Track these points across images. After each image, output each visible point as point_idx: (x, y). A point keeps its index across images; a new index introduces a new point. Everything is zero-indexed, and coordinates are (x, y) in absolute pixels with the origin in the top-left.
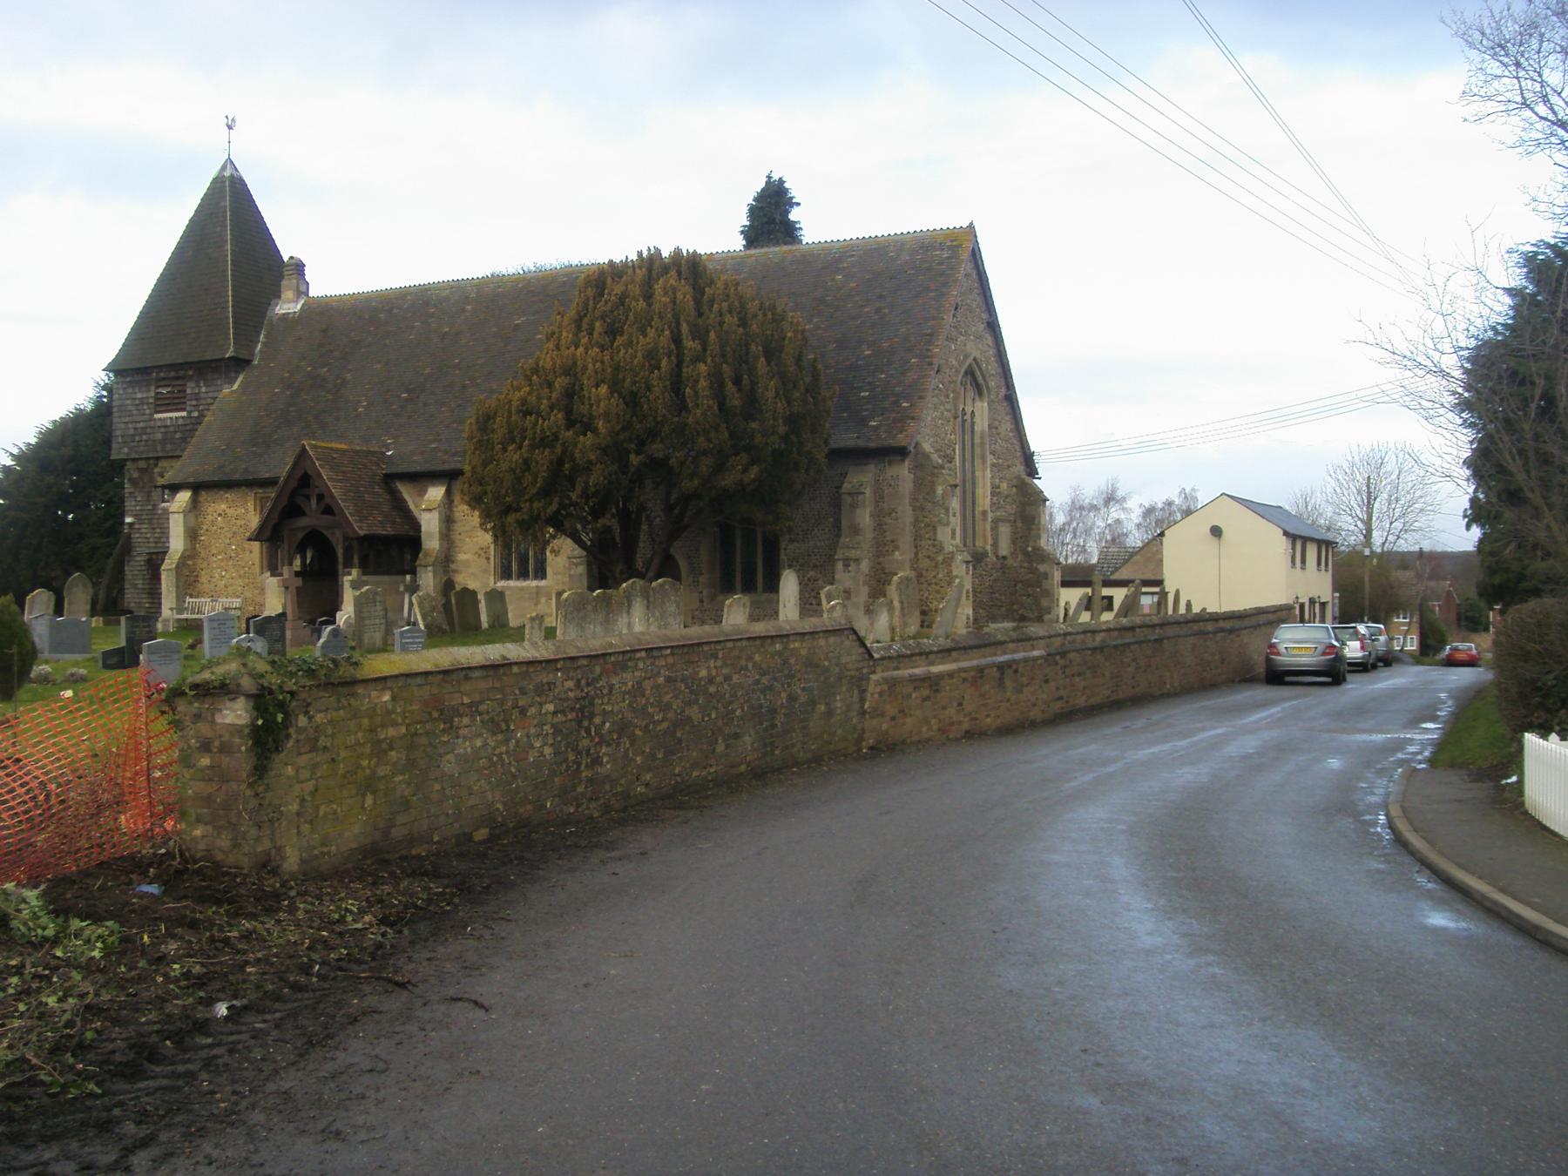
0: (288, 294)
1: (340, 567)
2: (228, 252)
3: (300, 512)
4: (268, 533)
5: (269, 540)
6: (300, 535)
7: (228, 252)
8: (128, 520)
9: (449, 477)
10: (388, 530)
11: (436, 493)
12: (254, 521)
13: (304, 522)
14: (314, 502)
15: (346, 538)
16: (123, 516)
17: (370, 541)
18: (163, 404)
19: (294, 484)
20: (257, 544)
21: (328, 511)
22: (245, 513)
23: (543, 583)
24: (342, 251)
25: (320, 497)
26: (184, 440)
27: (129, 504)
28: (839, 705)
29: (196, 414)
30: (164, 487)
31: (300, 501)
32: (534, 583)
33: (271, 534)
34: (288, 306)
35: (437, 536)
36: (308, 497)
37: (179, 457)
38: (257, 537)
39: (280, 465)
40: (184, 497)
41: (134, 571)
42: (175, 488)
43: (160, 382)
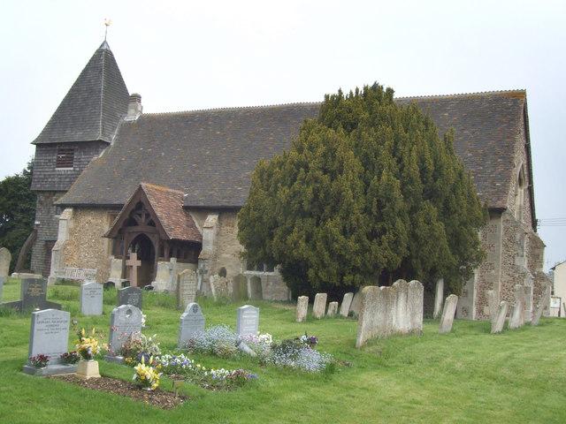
0: (131, 111)
1: (156, 256)
2: (101, 79)
3: (136, 224)
4: (115, 234)
5: (115, 238)
6: (134, 236)
7: (101, 79)
8: (37, 223)
9: (223, 211)
10: (184, 237)
11: (212, 219)
12: (107, 229)
13: (138, 229)
14: (143, 219)
15: (161, 240)
16: (34, 219)
17: (176, 242)
18: (61, 163)
19: (133, 207)
20: (107, 239)
21: (152, 224)
22: (104, 224)
23: (271, 274)
24: (159, 90)
25: (148, 216)
26: (71, 182)
27: (38, 215)
28: (524, 392)
29: (78, 169)
30: (58, 205)
31: (136, 218)
32: (267, 273)
33: (117, 236)
34: (132, 117)
35: (212, 242)
36: (140, 215)
37: (66, 191)
38: (108, 236)
39: (125, 198)
40: (68, 213)
41: (38, 249)
42: (63, 207)
43: (61, 151)
